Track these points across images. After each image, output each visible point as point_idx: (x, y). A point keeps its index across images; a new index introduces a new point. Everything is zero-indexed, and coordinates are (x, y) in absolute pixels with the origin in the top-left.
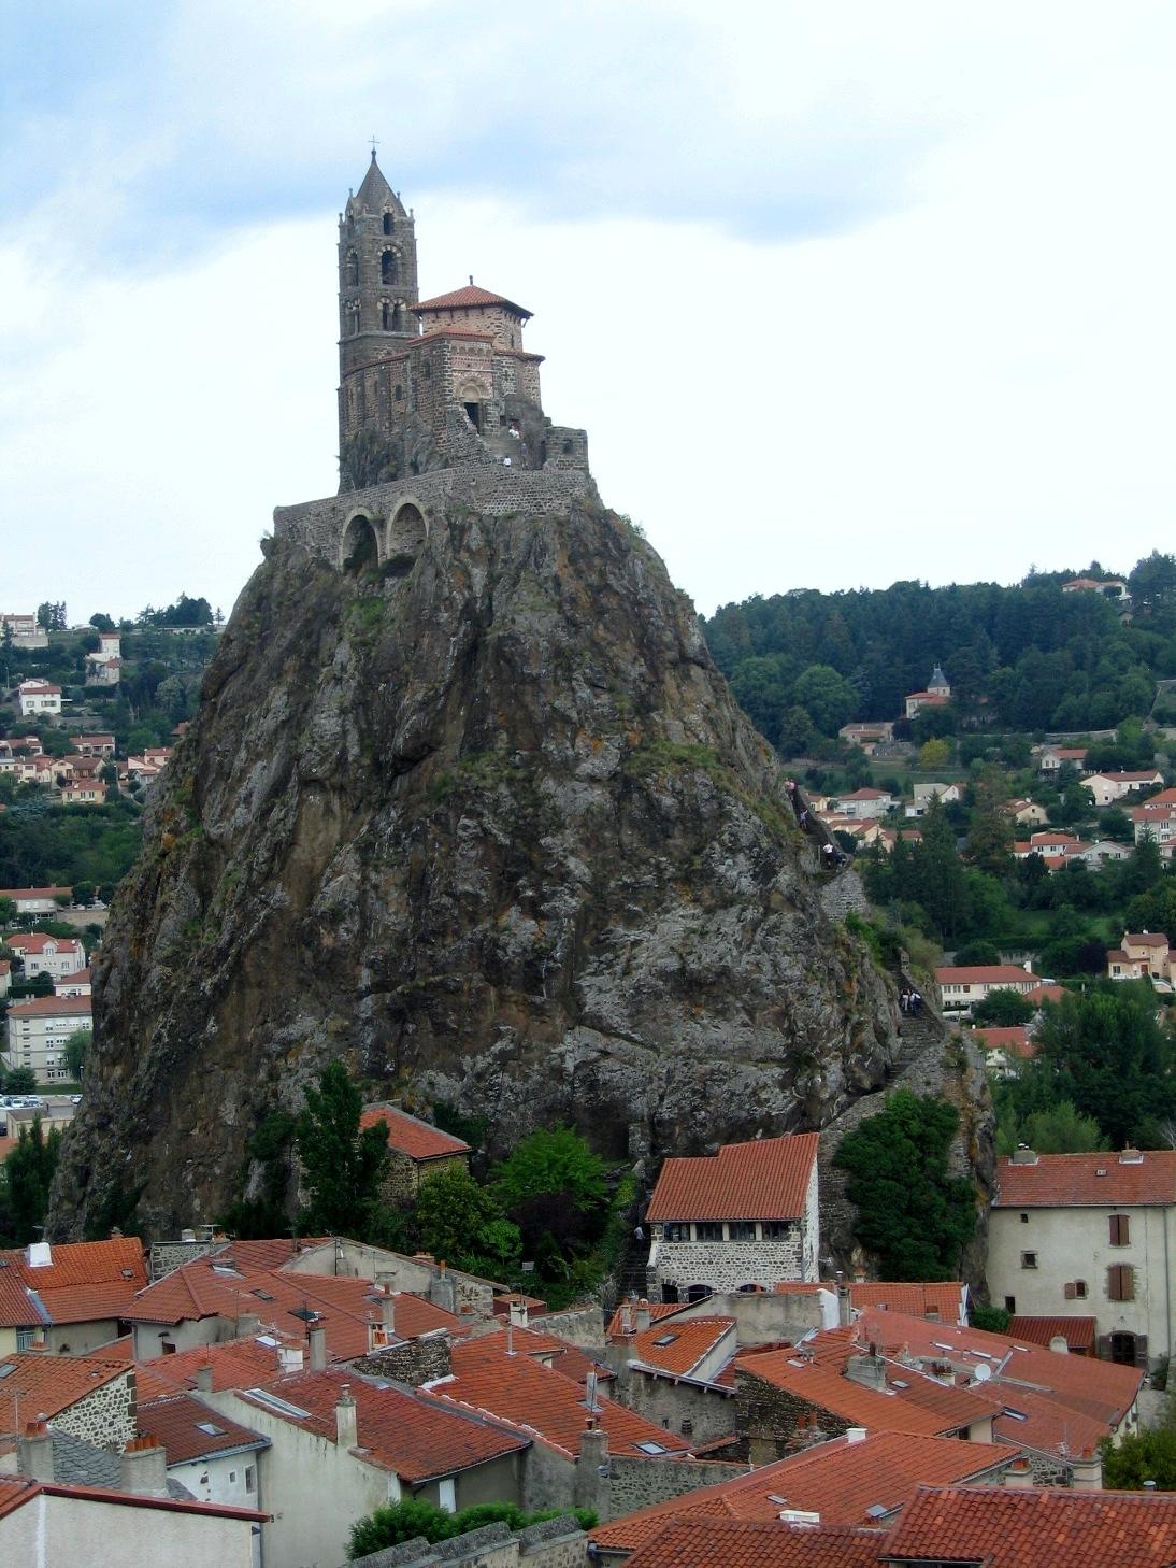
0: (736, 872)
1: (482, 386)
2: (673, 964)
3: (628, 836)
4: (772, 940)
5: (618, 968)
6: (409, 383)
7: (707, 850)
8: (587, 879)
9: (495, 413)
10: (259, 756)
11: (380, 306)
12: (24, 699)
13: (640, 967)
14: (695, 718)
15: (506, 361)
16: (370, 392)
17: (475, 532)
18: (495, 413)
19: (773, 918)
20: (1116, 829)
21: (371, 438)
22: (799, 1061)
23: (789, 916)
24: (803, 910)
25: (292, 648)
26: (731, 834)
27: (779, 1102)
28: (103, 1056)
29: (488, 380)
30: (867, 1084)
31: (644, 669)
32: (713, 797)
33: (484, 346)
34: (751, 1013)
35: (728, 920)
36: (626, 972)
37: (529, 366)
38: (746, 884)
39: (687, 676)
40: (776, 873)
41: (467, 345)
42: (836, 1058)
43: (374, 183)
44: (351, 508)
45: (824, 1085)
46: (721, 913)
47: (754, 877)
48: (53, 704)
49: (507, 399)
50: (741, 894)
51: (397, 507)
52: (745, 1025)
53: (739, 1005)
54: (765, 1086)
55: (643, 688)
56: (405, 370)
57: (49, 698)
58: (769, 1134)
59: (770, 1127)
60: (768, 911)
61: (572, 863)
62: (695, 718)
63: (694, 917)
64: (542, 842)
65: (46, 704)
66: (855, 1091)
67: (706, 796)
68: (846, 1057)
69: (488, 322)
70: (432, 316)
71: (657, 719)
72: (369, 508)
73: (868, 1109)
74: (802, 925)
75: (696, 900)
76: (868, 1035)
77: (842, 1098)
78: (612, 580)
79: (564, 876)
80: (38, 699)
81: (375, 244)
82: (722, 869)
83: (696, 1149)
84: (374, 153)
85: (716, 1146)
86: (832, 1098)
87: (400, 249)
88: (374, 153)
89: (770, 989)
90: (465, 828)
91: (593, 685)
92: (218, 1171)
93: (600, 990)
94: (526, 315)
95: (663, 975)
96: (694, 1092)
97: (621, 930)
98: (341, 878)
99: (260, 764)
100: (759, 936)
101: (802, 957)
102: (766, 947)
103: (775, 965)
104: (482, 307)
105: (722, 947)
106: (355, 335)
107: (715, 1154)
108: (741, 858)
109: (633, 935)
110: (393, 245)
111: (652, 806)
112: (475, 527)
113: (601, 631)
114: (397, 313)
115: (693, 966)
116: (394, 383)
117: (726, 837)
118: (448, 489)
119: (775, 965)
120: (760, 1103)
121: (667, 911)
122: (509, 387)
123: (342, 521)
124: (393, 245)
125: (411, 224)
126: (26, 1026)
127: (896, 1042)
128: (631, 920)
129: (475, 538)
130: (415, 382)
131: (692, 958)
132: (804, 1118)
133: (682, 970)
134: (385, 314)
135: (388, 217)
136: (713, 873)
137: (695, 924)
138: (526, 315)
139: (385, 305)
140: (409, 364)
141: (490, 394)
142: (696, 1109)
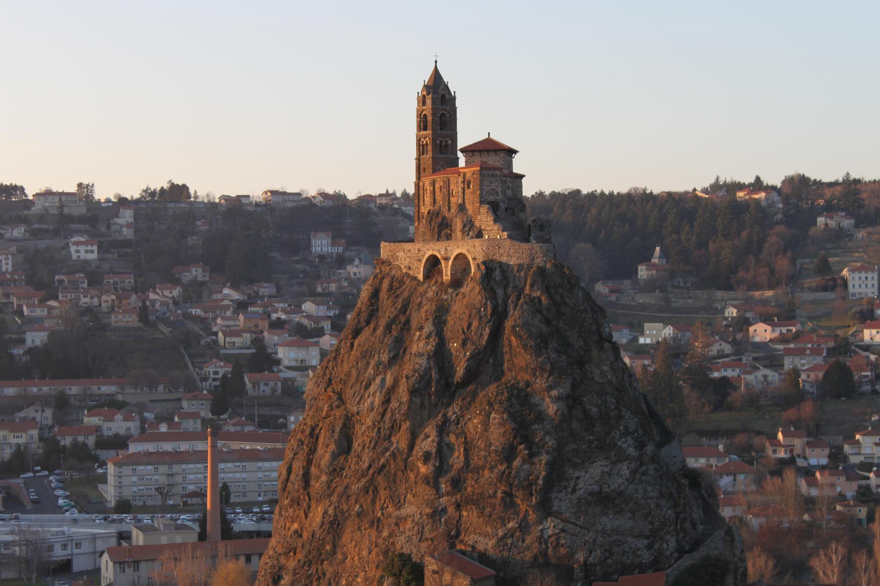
0: (628, 446)
1: (497, 193)
2: (596, 488)
3: (575, 425)
4: (644, 478)
5: (570, 490)
6: (460, 189)
7: (613, 434)
9: (503, 206)
10: (380, 373)
11: (438, 142)
12: (73, 249)
13: (580, 489)
14: (606, 368)
15: (508, 179)
16: (437, 190)
17: (498, 271)
18: (503, 206)
19: (644, 468)
20: (773, 361)
22: (654, 536)
23: (651, 467)
24: (658, 464)
26: (625, 427)
27: (646, 557)
28: (286, 518)
29: (499, 190)
30: (687, 548)
31: (582, 344)
32: (616, 408)
33: (498, 173)
34: (633, 513)
35: (625, 469)
36: (574, 491)
37: (518, 181)
38: (631, 451)
39: (602, 348)
40: (645, 446)
41: (490, 173)
42: (673, 535)
43: (436, 76)
44: (428, 250)
45: (667, 549)
46: (619, 465)
47: (635, 447)
48: (92, 252)
49: (509, 199)
50: (629, 455)
51: (455, 254)
52: (630, 518)
53: (627, 509)
54: (639, 549)
55: (582, 352)
56: (457, 182)
57: (89, 248)
58: (641, 571)
59: (642, 568)
60: (642, 464)
62: (606, 368)
63: (606, 466)
64: (533, 427)
65: (87, 252)
66: (681, 552)
67: (613, 407)
68: (678, 535)
69: (498, 158)
71: (588, 368)
72: (439, 251)
73: (687, 561)
74: (658, 471)
75: (607, 458)
76: (687, 525)
77: (676, 555)
78: (567, 300)
80: (82, 248)
81: (438, 107)
82: (620, 443)
83: (606, 577)
85: (616, 576)
86: (671, 555)
87: (448, 112)
89: (642, 502)
90: (494, 419)
91: (558, 352)
92: (359, 580)
93: (561, 500)
94: (515, 152)
95: (591, 493)
96: (606, 550)
97: (571, 471)
98: (430, 439)
99: (380, 377)
100: (637, 476)
101: (657, 487)
102: (641, 482)
103: (645, 490)
104: (496, 151)
105: (620, 481)
107: (617, 580)
108: (629, 438)
110: (445, 110)
111: (586, 412)
112: (498, 270)
113: (561, 324)
114: (446, 145)
117: (622, 427)
119: (645, 490)
120: (638, 556)
121: (593, 462)
122: (509, 193)
124: (445, 110)
125: (454, 99)
126: (120, 470)
127: (700, 528)
128: (575, 466)
129: (497, 274)
130: (464, 190)
131: (606, 486)
132: (656, 565)
133: (600, 492)
134: (441, 146)
135: (443, 96)
136: (616, 445)
137: (607, 469)
138: (515, 152)
139: (441, 142)
141: (500, 197)
142: (607, 558)
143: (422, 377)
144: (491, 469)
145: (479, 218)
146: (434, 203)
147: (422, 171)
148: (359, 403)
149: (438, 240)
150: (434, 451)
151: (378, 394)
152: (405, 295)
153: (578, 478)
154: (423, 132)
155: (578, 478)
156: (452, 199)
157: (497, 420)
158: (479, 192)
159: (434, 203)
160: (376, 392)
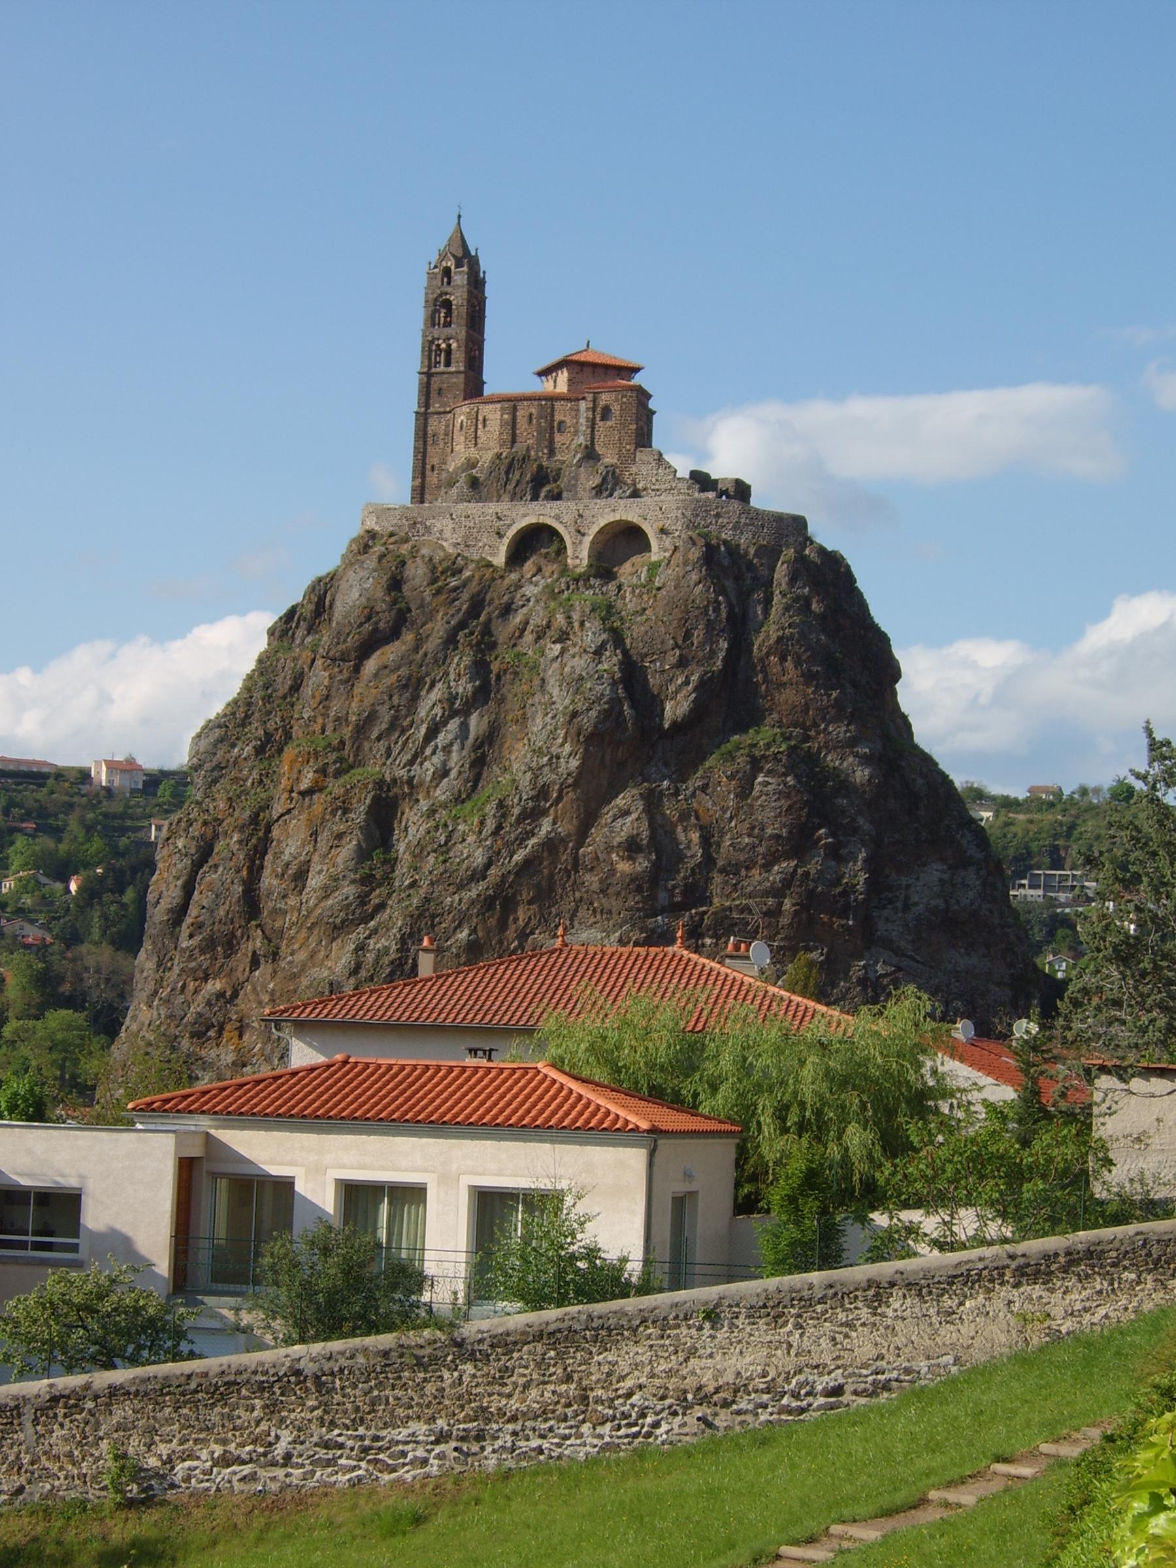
2: (939, 903)
5: (899, 904)
6: (582, 421)
8: (873, 833)
13: (916, 904)
21: (524, 459)
25: (462, 625)
36: (906, 907)
44: (524, 516)
47: (978, 846)
52: (984, 956)
61: (861, 821)
70: (577, 369)
72: (557, 518)
79: (855, 830)
84: (459, 217)
88: (459, 217)
97: (894, 876)
106: (442, 368)
109: (904, 881)
115: (956, 907)
116: (558, 417)
118: (688, 514)
121: (925, 865)
123: (510, 526)
131: (953, 901)
140: (583, 405)
143: (605, 715)
144: (767, 867)
145: (634, 469)
146: (514, 442)
147: (433, 395)
148: (411, 763)
149: (532, 500)
150: (645, 834)
151: (455, 748)
152: (473, 587)
153: (908, 887)
154: (436, 332)
155: (908, 887)
156: (558, 438)
157: (770, 787)
158: (634, 427)
159: (514, 442)
160: (451, 744)
